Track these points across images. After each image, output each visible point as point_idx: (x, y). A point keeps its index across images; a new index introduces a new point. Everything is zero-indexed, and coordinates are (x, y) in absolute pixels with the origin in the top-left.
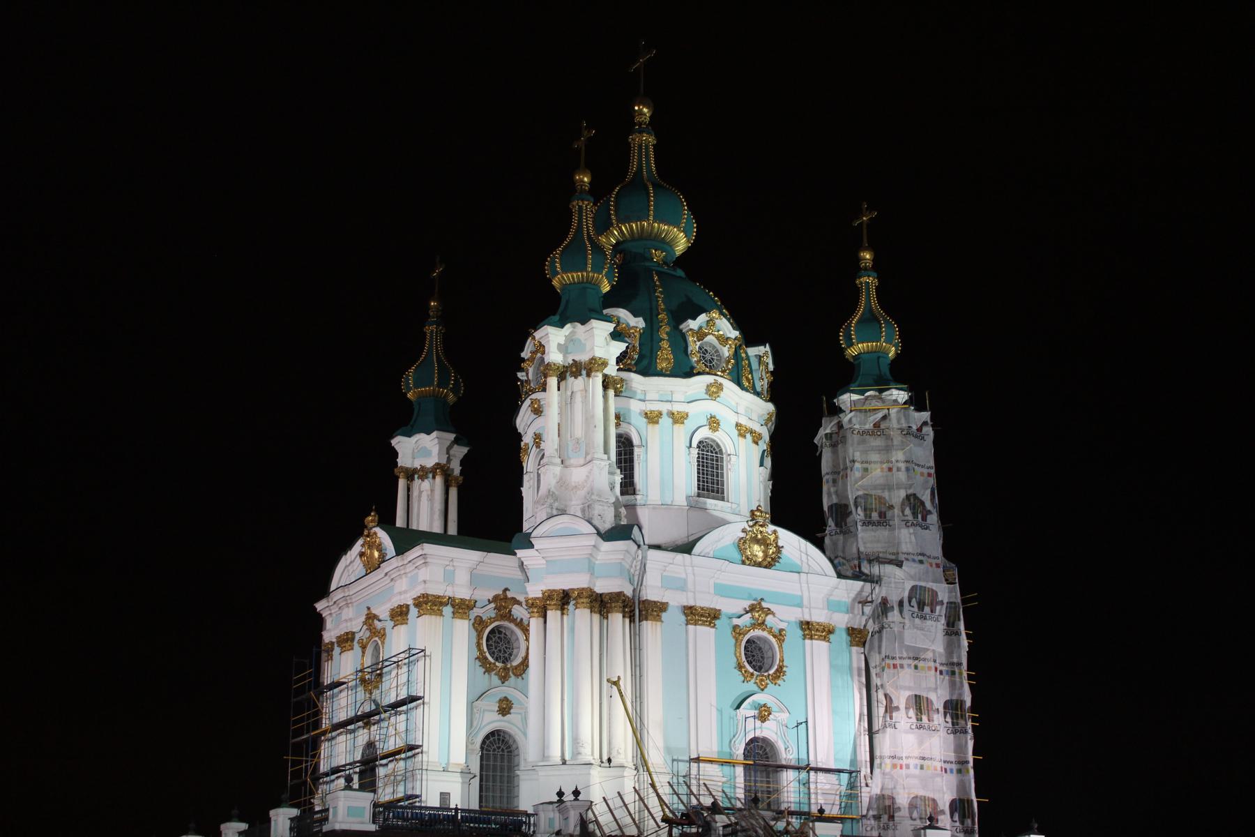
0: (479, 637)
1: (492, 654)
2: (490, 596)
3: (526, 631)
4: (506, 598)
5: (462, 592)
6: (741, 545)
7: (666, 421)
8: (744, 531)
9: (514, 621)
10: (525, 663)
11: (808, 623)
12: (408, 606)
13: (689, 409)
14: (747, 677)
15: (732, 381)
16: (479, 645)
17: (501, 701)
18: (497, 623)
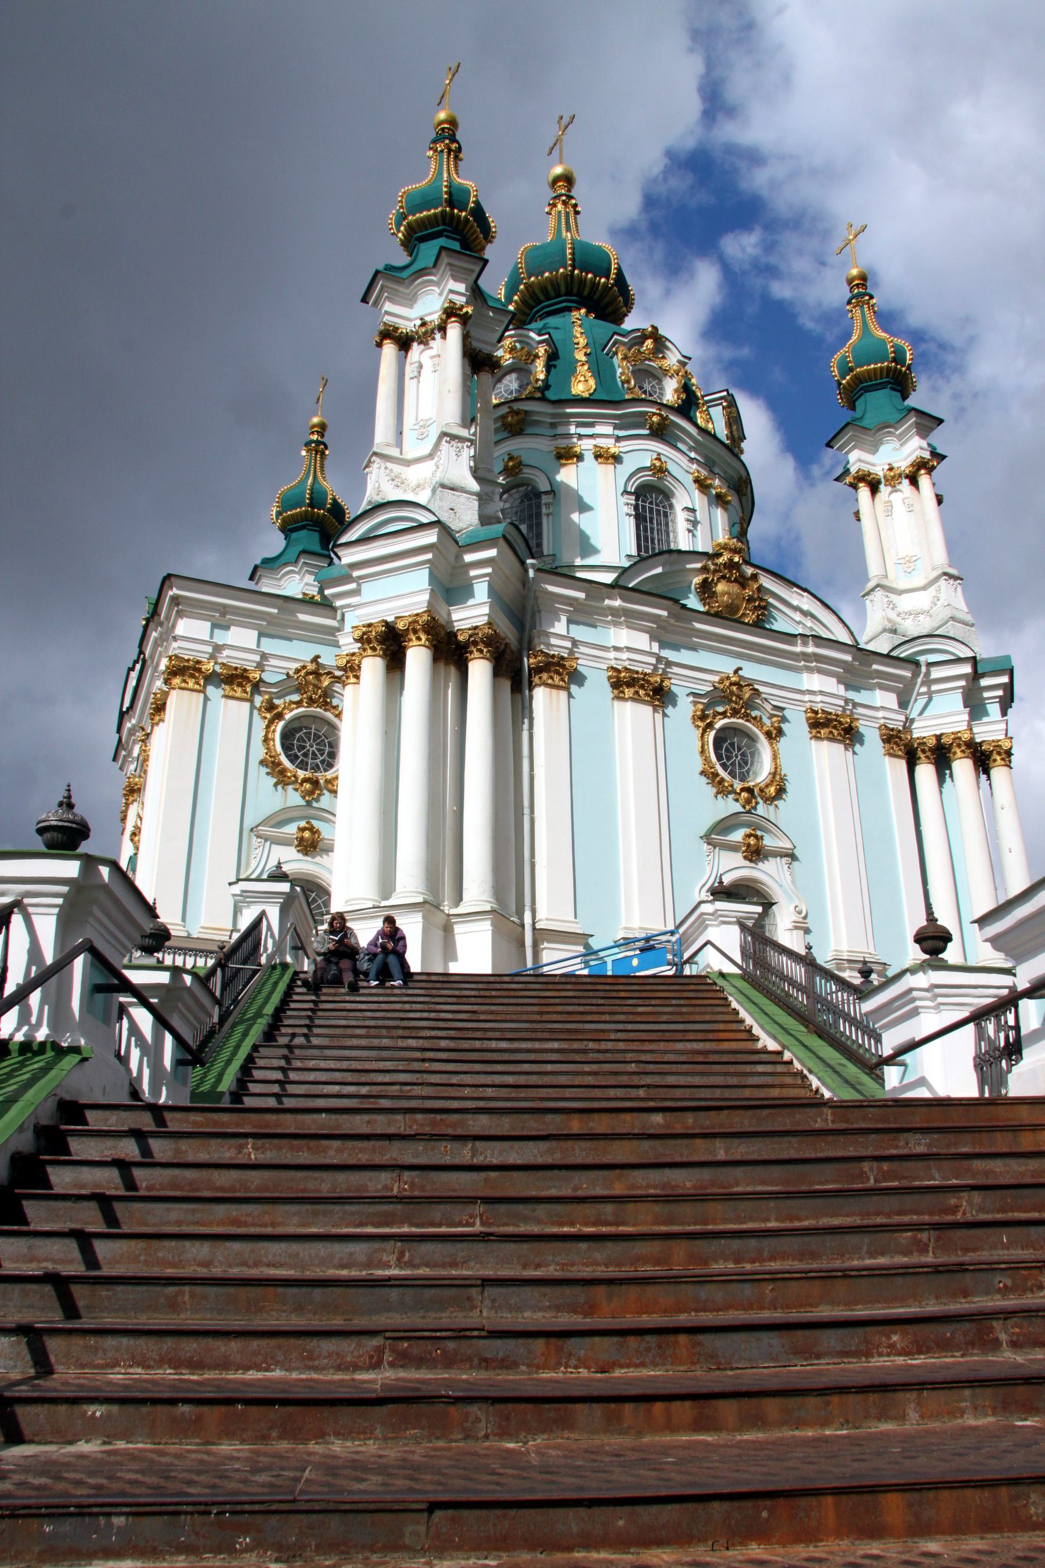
1: (292, 759)
8: (705, 569)
11: (816, 713)
14: (722, 790)
16: (266, 740)
17: (302, 830)
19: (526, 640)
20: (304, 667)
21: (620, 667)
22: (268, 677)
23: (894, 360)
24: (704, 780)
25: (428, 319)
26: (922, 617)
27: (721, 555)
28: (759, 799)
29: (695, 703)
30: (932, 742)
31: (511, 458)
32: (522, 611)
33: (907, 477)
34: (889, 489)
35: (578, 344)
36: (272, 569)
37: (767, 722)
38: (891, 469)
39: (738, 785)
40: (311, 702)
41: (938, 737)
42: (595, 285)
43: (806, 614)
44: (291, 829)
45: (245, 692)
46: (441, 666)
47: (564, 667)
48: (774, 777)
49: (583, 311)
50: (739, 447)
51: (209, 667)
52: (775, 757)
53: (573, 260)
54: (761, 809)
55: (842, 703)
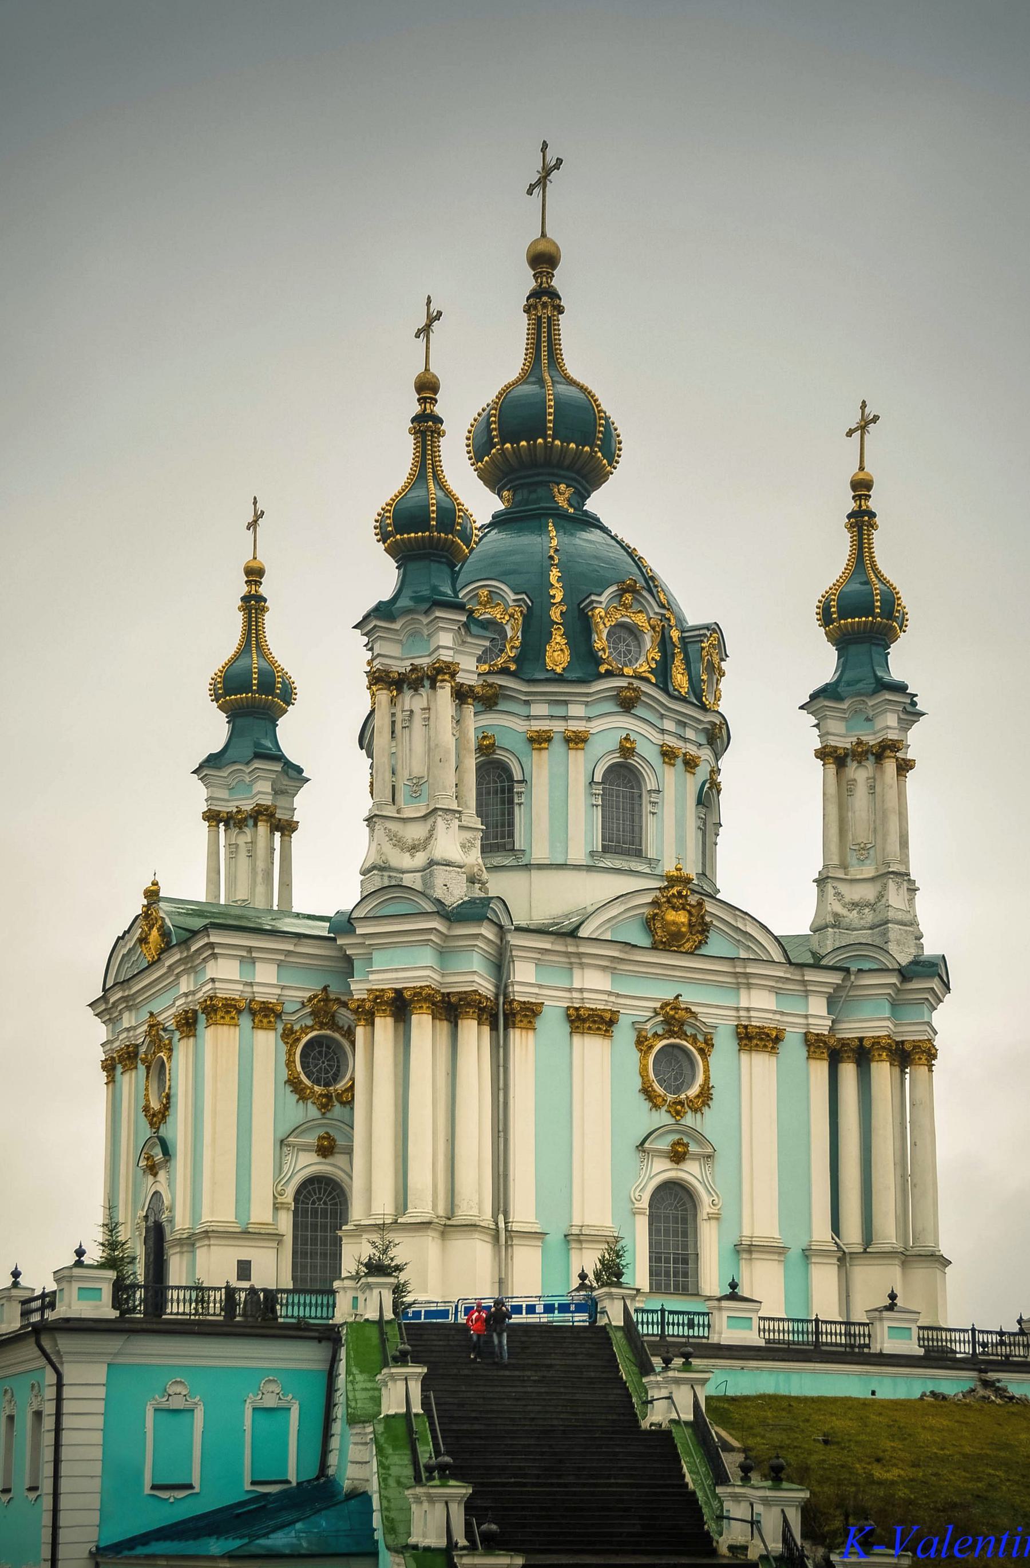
0: (290, 1053)
2: (308, 994)
3: (353, 1043)
4: (326, 1000)
5: (266, 994)
6: (649, 924)
7: (558, 746)
8: (655, 903)
9: (337, 1028)
10: (352, 1088)
11: (746, 1027)
12: (195, 1012)
15: (655, 685)
16: (290, 1063)
17: (321, 1138)
18: (315, 1033)
20: (315, 996)
21: (577, 1006)
22: (289, 1008)
24: (643, 1097)
25: (417, 662)
26: (867, 910)
27: (673, 887)
28: (689, 1111)
29: (639, 1031)
31: (484, 738)
32: (500, 964)
33: (873, 754)
34: (855, 764)
37: (700, 1038)
38: (860, 743)
39: (670, 1098)
41: (861, 1039)
43: (746, 933)
44: (311, 1139)
45: (270, 1022)
46: (437, 1022)
47: (532, 1011)
48: (703, 1089)
50: (720, 669)
51: (243, 1004)
52: (707, 1070)
54: (689, 1119)
55: (770, 1016)
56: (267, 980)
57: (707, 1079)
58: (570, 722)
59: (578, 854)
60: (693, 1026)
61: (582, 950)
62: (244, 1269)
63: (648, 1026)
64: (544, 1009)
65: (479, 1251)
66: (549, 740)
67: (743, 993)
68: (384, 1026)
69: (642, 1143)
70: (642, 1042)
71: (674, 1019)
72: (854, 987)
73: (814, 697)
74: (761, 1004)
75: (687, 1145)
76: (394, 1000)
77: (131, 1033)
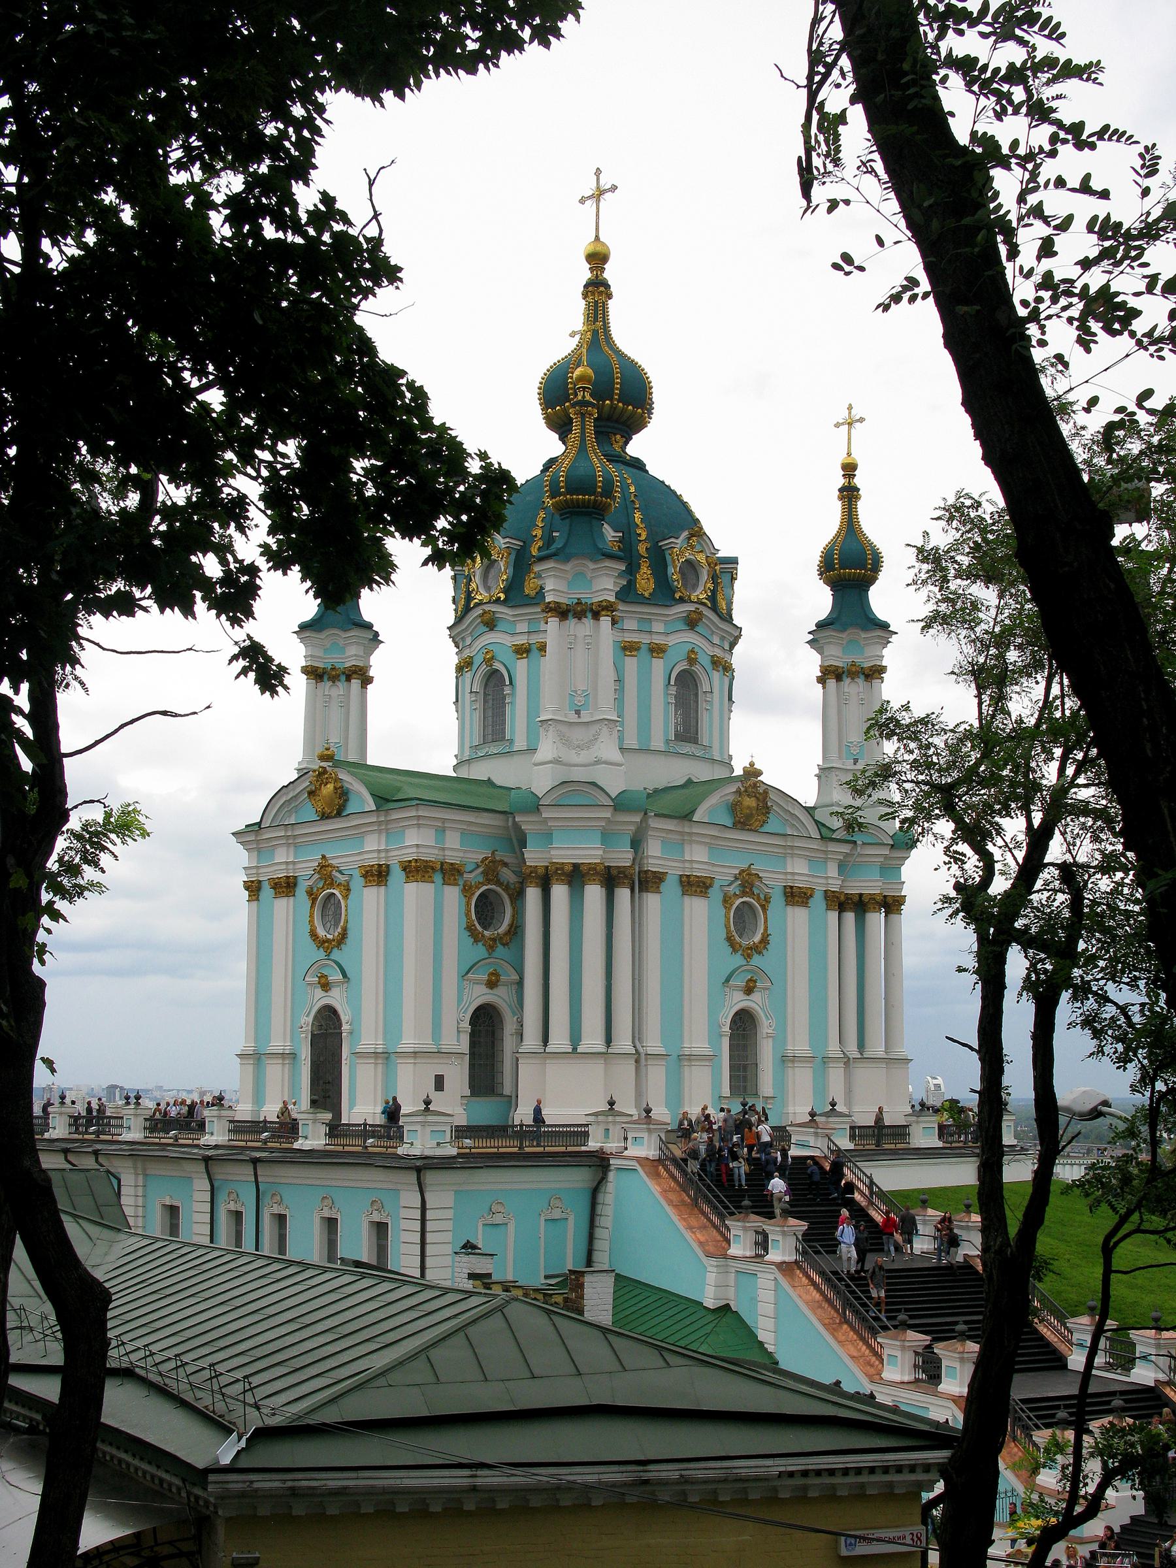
0: (468, 904)
6: (734, 808)
8: (738, 792)
9: (499, 883)
11: (791, 887)
12: (388, 866)
13: (672, 640)
16: (468, 914)
17: (492, 974)
18: (485, 888)
19: (637, 861)
20: (486, 858)
23: (871, 570)
30: (856, 898)
34: (847, 681)
35: (640, 535)
36: (320, 630)
37: (762, 896)
40: (489, 881)
41: (861, 895)
42: (633, 414)
49: (618, 437)
53: (619, 395)
54: (756, 960)
56: (455, 847)
57: (766, 929)
58: (654, 636)
59: (658, 743)
60: (759, 888)
61: (694, 831)
62: (439, 1082)
63: (731, 888)
64: (668, 878)
65: (627, 1069)
66: (638, 649)
67: (789, 860)
68: (559, 892)
69: (727, 980)
70: (727, 901)
71: (747, 881)
72: (861, 855)
73: (821, 625)
74: (799, 871)
75: (755, 981)
76: (573, 871)
77: (291, 867)
